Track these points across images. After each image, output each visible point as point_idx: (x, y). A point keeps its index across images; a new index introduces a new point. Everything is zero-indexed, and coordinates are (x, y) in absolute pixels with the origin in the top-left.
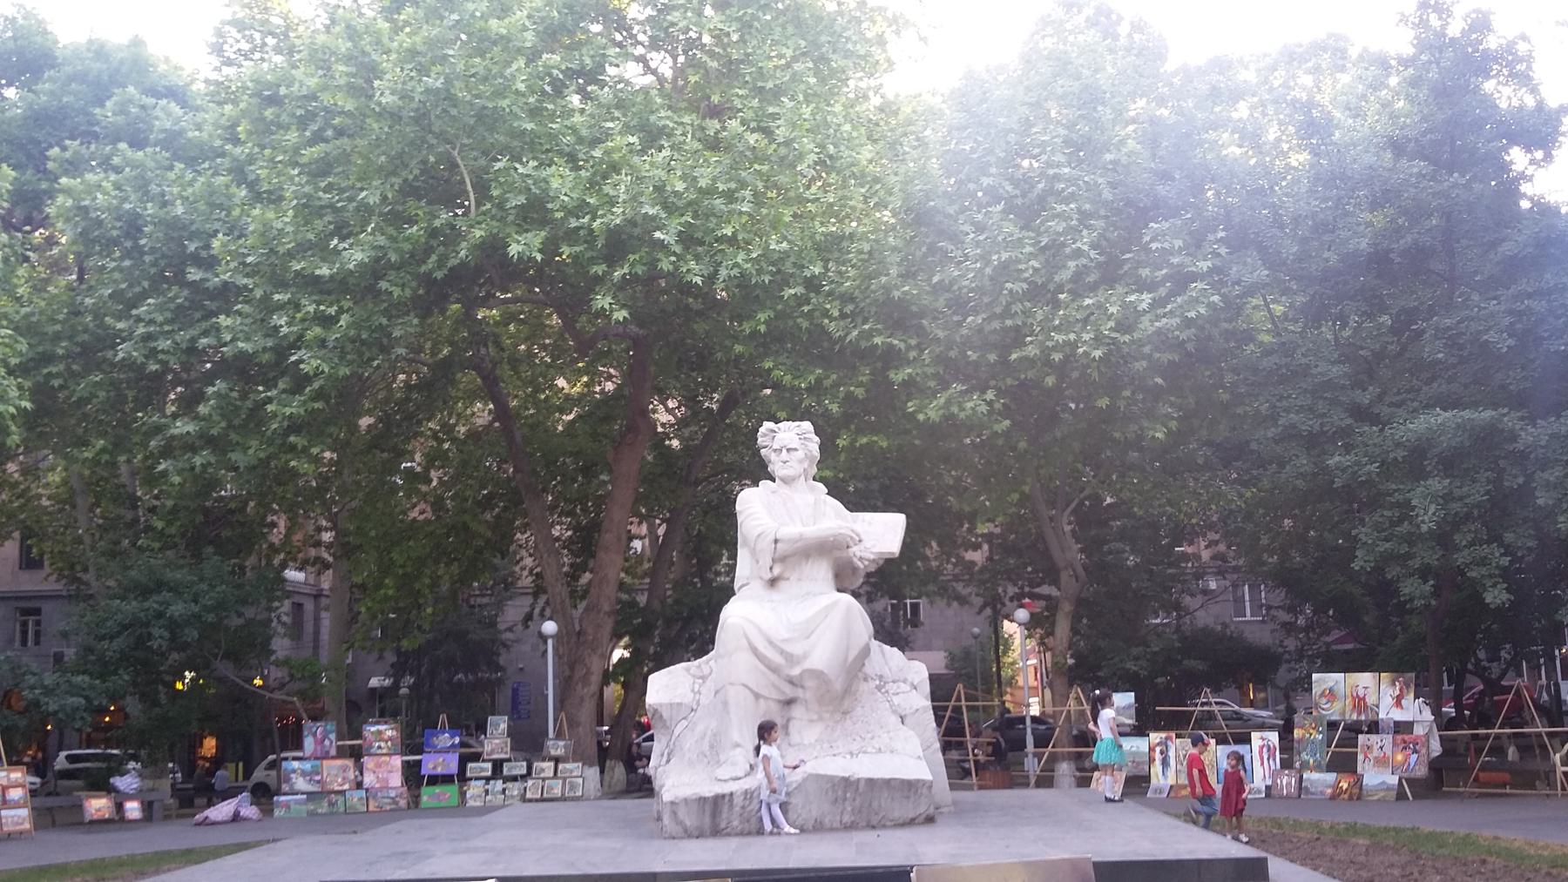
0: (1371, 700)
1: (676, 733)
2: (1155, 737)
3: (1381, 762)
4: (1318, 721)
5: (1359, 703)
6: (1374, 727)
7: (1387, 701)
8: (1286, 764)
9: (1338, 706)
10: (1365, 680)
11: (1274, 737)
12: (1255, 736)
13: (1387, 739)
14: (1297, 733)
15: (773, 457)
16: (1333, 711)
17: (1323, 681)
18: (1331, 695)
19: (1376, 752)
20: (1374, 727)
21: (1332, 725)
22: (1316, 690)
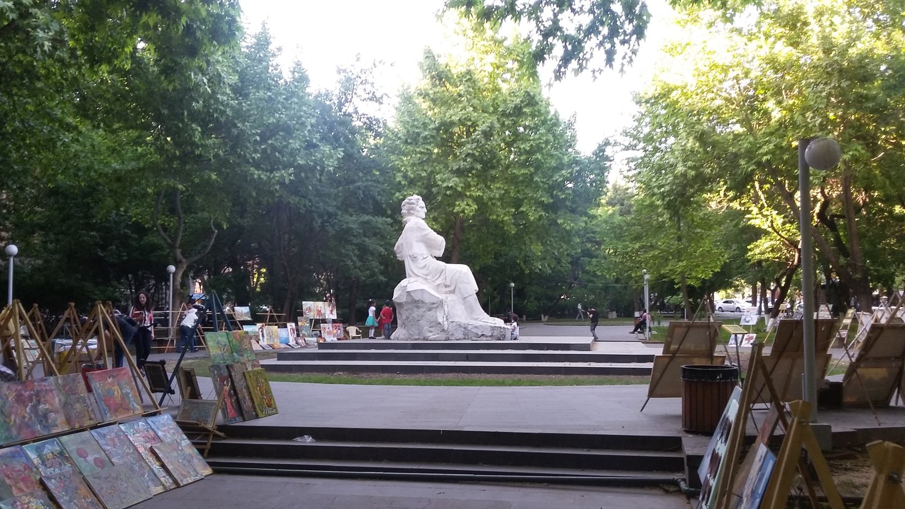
0: (323, 312)
1: (446, 307)
2: (259, 325)
3: (329, 333)
4: (306, 318)
5: (319, 312)
6: (324, 321)
7: (328, 312)
8: (298, 335)
9: (312, 313)
10: (320, 304)
11: (293, 324)
12: (288, 324)
13: (330, 325)
14: (300, 324)
15: (418, 208)
16: (312, 315)
17: (306, 304)
18: (310, 309)
19: (327, 330)
20: (324, 321)
21: (311, 320)
22: (304, 308)
